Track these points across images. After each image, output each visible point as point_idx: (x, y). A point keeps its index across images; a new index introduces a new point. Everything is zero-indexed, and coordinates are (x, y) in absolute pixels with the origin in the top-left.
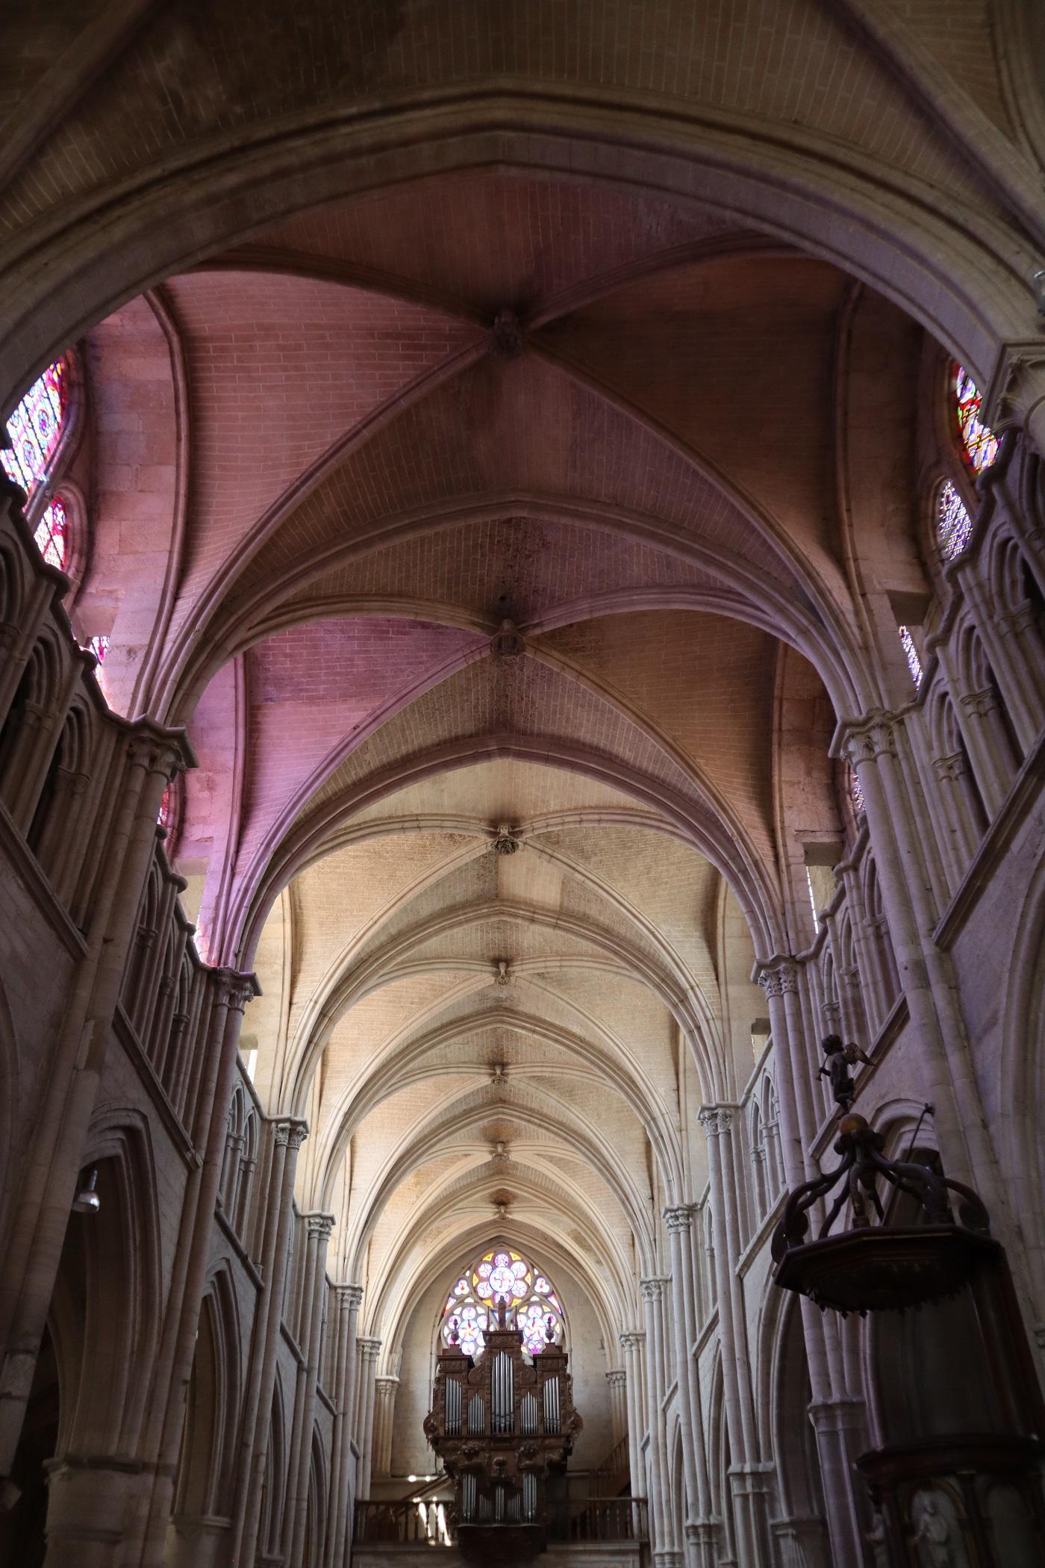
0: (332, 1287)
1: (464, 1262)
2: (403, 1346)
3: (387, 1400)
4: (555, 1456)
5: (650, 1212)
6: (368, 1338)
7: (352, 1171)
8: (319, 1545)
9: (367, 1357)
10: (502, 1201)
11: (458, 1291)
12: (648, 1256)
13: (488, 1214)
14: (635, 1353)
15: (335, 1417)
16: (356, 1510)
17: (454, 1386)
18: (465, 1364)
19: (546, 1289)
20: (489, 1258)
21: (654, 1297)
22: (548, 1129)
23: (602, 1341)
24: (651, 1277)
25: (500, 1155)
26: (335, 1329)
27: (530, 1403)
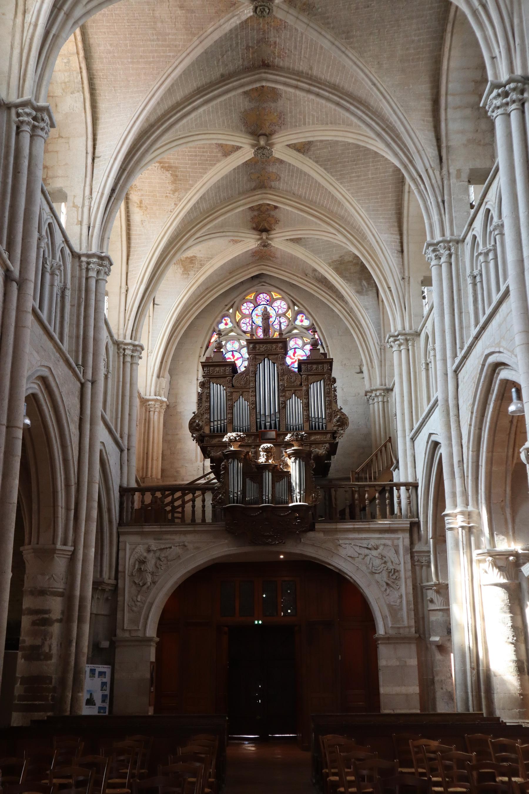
0: (76, 256)
1: (228, 300)
2: (170, 372)
3: (157, 419)
4: (321, 451)
5: (437, 173)
6: (128, 340)
7: (94, 140)
8: (68, 509)
9: (128, 359)
10: (263, 222)
11: (222, 326)
12: (435, 218)
13: (250, 243)
14: (403, 352)
15: (83, 385)
16: (121, 496)
17: (218, 391)
18: (228, 369)
19: (306, 323)
20: (252, 297)
21: (443, 259)
22: (318, 95)
23: (361, 366)
24: (438, 238)
25: (263, 148)
26: (79, 297)
27: (295, 405)
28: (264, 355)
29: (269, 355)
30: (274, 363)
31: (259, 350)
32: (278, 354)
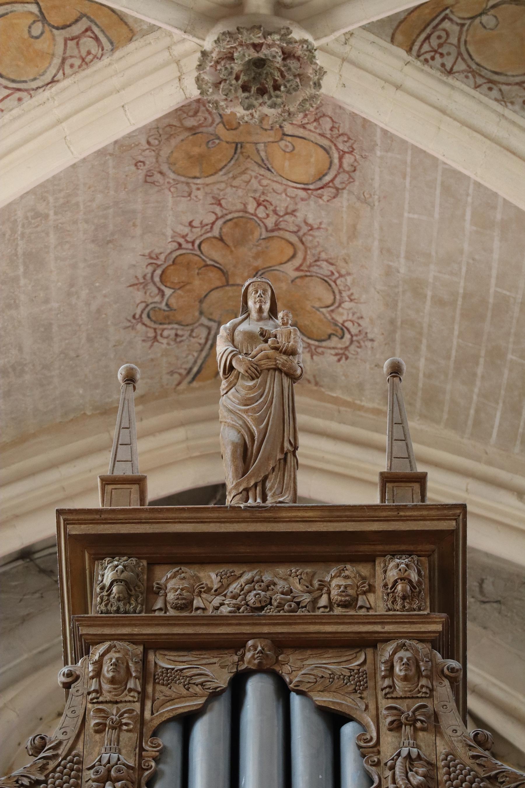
28: (237, 645)
29: (281, 644)
30: (334, 721)
31: (186, 605)
32: (370, 643)
